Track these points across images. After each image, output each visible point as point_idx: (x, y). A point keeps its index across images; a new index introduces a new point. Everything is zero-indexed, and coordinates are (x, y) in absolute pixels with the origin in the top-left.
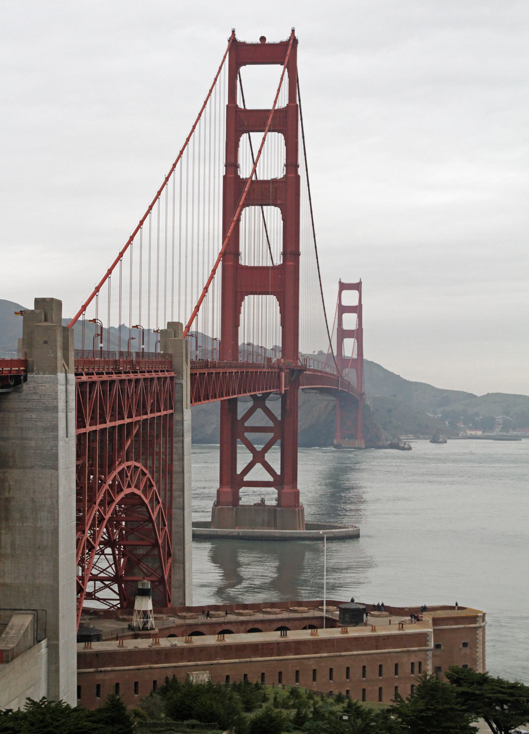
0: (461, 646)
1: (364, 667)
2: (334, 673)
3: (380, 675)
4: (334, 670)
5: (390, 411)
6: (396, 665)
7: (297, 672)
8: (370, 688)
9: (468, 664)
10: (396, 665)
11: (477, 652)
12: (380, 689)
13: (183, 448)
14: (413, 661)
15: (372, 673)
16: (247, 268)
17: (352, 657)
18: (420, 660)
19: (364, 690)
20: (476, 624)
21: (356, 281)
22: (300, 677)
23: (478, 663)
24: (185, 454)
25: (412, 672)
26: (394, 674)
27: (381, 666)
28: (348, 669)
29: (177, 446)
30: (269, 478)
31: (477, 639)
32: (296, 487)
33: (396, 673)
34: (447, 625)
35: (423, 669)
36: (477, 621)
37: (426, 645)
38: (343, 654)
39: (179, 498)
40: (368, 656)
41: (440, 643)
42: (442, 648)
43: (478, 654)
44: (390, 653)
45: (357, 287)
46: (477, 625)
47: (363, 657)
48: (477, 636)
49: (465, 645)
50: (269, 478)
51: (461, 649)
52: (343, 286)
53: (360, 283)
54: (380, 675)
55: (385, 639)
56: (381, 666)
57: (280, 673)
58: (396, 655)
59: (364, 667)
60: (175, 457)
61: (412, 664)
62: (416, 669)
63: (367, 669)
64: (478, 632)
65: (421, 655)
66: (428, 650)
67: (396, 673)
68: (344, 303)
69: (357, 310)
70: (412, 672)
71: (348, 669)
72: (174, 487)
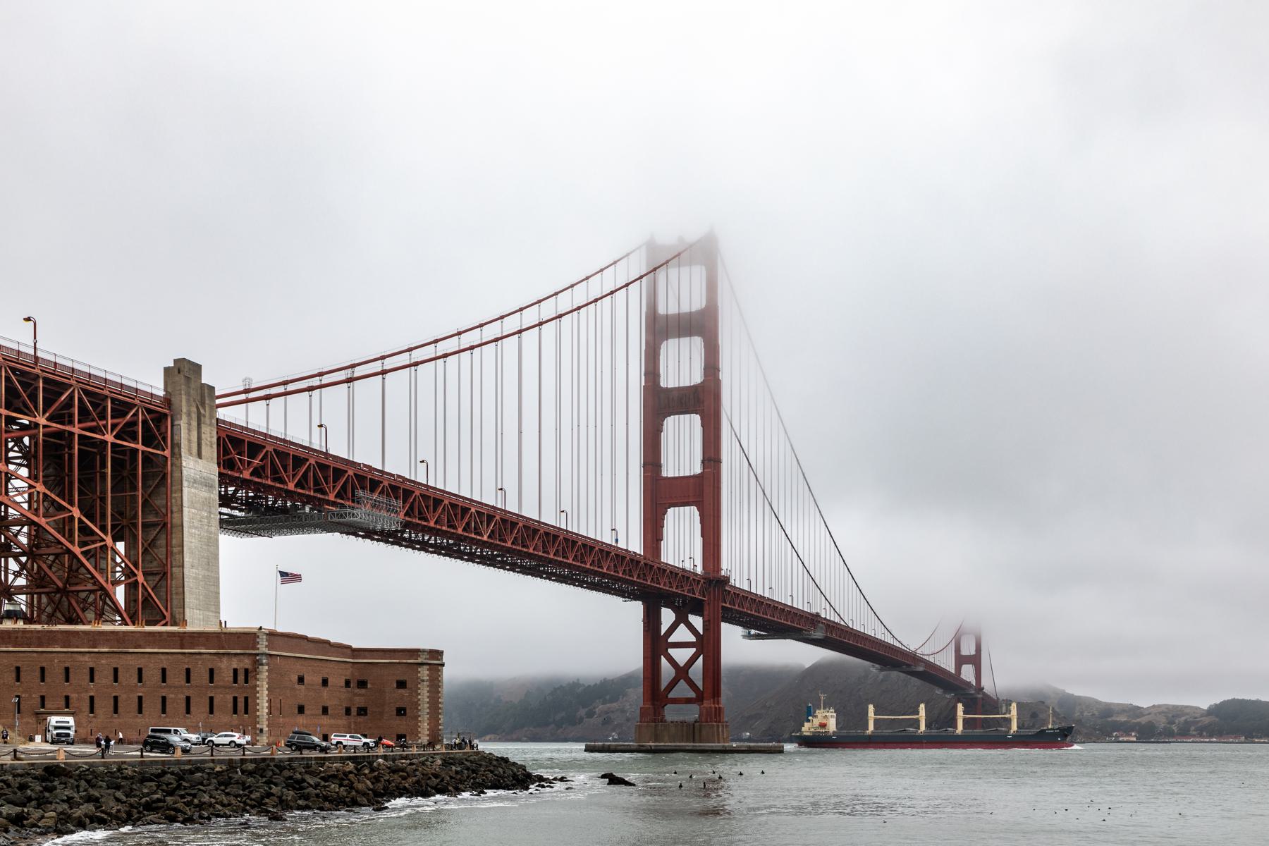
3: (188, 681)
6: (211, 671)
7: (67, 669)
8: (172, 696)
10: (211, 671)
12: (188, 699)
13: (182, 497)
14: (235, 666)
15: (176, 678)
19: (164, 699)
22: (71, 675)
24: (185, 504)
25: (235, 681)
26: (208, 682)
27: (188, 671)
29: (176, 495)
33: (211, 681)
38: (131, 650)
44: (200, 654)
54: (188, 681)
55: (194, 637)
56: (188, 671)
57: (43, 669)
58: (208, 656)
61: (235, 671)
62: (241, 677)
67: (211, 681)
70: (235, 681)
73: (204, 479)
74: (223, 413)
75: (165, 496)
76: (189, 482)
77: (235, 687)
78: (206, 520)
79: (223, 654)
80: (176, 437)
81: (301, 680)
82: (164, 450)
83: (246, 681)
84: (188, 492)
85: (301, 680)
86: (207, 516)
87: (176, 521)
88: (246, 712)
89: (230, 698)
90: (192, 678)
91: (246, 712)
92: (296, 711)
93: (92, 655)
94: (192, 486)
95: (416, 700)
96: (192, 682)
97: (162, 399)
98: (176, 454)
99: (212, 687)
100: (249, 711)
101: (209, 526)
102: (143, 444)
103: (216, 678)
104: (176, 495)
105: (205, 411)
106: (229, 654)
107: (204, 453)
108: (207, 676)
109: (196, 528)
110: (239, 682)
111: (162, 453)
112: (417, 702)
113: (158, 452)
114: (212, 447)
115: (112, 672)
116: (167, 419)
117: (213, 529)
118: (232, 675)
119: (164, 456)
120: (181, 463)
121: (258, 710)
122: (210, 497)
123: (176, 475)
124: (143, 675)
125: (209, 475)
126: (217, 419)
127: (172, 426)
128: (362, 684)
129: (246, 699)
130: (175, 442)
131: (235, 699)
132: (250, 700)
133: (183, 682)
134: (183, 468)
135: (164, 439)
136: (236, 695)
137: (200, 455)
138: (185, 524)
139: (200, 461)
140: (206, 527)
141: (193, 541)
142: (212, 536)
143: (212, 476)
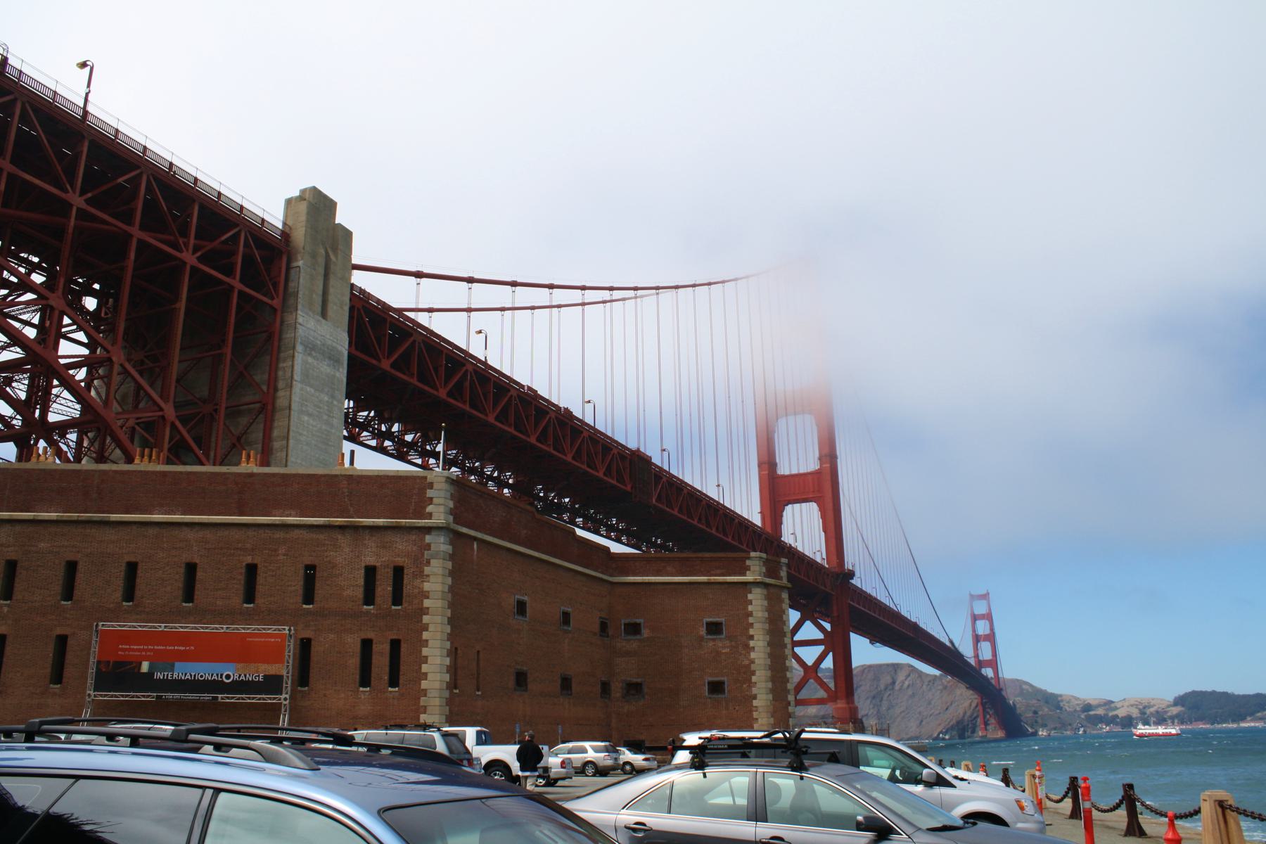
0: (703, 631)
1: (191, 569)
2: (81, 577)
4: (80, 567)
5: (1035, 712)
9: (725, 679)
11: (750, 649)
14: (370, 560)
16: (784, 476)
17: (152, 531)
18: (400, 561)
20: (744, 575)
21: (983, 592)
23: (754, 679)
25: (369, 598)
26: (300, 599)
27: (252, 570)
28: (132, 568)
29: (285, 365)
30: (822, 694)
31: (751, 614)
32: (853, 702)
33: (309, 597)
34: (658, 573)
35: (407, 589)
36: (748, 568)
37: (421, 514)
39: (282, 450)
40: (208, 534)
41: (638, 621)
42: (646, 633)
43: (753, 655)
45: (985, 597)
46: (749, 578)
47: (190, 535)
48: (750, 608)
49: (715, 628)
50: (822, 694)
51: (701, 638)
52: (972, 597)
53: (988, 594)
56: (252, 570)
58: (304, 534)
59: (191, 569)
60: (281, 384)
61: (371, 572)
62: (384, 588)
63: (200, 574)
64: (750, 597)
65: (402, 547)
66: (429, 530)
67: (309, 597)
68: (977, 612)
69: (988, 617)
71: (132, 568)
72: (276, 433)
73: (328, 348)
74: (358, 278)
75: (267, 368)
76: (306, 347)
77: (368, 612)
78: (326, 408)
79: (342, 528)
80: (292, 285)
81: (521, 608)
82: (273, 298)
83: (397, 598)
84: (300, 359)
85: (521, 608)
86: (327, 402)
87: (281, 401)
88: (394, 682)
89: (353, 643)
90: (261, 588)
91: (394, 682)
92: (511, 683)
93: (18, 528)
94: (310, 354)
95: (746, 662)
96: (260, 600)
97: (279, 233)
98: (287, 299)
99: (308, 612)
100: (402, 680)
101: (329, 416)
102: (242, 281)
103: (320, 592)
104: (285, 365)
105: (337, 259)
106: (356, 528)
107: (330, 313)
108: (297, 585)
109: (310, 415)
110: (378, 600)
111: (269, 301)
112: (748, 666)
113: (265, 299)
114: (342, 308)
115: (61, 572)
116: (281, 258)
117: (335, 421)
118: (361, 582)
119: (271, 306)
120: (296, 319)
121: (425, 676)
122: (334, 376)
123: (288, 336)
124: (138, 580)
125: (334, 344)
126: (352, 285)
127: (288, 269)
128: (634, 629)
129: (395, 645)
130: (291, 290)
131: (367, 645)
132: (404, 648)
133: (236, 600)
134: (298, 326)
135: (275, 285)
136: (370, 635)
137: (324, 314)
138: (294, 406)
139: (324, 321)
140: (325, 417)
141: (305, 433)
142: (333, 431)
143: (340, 348)
